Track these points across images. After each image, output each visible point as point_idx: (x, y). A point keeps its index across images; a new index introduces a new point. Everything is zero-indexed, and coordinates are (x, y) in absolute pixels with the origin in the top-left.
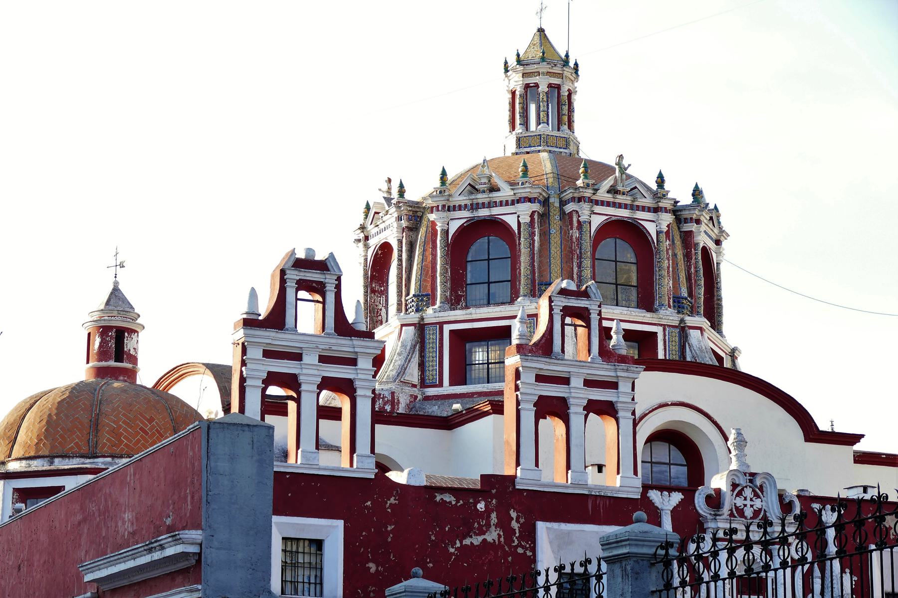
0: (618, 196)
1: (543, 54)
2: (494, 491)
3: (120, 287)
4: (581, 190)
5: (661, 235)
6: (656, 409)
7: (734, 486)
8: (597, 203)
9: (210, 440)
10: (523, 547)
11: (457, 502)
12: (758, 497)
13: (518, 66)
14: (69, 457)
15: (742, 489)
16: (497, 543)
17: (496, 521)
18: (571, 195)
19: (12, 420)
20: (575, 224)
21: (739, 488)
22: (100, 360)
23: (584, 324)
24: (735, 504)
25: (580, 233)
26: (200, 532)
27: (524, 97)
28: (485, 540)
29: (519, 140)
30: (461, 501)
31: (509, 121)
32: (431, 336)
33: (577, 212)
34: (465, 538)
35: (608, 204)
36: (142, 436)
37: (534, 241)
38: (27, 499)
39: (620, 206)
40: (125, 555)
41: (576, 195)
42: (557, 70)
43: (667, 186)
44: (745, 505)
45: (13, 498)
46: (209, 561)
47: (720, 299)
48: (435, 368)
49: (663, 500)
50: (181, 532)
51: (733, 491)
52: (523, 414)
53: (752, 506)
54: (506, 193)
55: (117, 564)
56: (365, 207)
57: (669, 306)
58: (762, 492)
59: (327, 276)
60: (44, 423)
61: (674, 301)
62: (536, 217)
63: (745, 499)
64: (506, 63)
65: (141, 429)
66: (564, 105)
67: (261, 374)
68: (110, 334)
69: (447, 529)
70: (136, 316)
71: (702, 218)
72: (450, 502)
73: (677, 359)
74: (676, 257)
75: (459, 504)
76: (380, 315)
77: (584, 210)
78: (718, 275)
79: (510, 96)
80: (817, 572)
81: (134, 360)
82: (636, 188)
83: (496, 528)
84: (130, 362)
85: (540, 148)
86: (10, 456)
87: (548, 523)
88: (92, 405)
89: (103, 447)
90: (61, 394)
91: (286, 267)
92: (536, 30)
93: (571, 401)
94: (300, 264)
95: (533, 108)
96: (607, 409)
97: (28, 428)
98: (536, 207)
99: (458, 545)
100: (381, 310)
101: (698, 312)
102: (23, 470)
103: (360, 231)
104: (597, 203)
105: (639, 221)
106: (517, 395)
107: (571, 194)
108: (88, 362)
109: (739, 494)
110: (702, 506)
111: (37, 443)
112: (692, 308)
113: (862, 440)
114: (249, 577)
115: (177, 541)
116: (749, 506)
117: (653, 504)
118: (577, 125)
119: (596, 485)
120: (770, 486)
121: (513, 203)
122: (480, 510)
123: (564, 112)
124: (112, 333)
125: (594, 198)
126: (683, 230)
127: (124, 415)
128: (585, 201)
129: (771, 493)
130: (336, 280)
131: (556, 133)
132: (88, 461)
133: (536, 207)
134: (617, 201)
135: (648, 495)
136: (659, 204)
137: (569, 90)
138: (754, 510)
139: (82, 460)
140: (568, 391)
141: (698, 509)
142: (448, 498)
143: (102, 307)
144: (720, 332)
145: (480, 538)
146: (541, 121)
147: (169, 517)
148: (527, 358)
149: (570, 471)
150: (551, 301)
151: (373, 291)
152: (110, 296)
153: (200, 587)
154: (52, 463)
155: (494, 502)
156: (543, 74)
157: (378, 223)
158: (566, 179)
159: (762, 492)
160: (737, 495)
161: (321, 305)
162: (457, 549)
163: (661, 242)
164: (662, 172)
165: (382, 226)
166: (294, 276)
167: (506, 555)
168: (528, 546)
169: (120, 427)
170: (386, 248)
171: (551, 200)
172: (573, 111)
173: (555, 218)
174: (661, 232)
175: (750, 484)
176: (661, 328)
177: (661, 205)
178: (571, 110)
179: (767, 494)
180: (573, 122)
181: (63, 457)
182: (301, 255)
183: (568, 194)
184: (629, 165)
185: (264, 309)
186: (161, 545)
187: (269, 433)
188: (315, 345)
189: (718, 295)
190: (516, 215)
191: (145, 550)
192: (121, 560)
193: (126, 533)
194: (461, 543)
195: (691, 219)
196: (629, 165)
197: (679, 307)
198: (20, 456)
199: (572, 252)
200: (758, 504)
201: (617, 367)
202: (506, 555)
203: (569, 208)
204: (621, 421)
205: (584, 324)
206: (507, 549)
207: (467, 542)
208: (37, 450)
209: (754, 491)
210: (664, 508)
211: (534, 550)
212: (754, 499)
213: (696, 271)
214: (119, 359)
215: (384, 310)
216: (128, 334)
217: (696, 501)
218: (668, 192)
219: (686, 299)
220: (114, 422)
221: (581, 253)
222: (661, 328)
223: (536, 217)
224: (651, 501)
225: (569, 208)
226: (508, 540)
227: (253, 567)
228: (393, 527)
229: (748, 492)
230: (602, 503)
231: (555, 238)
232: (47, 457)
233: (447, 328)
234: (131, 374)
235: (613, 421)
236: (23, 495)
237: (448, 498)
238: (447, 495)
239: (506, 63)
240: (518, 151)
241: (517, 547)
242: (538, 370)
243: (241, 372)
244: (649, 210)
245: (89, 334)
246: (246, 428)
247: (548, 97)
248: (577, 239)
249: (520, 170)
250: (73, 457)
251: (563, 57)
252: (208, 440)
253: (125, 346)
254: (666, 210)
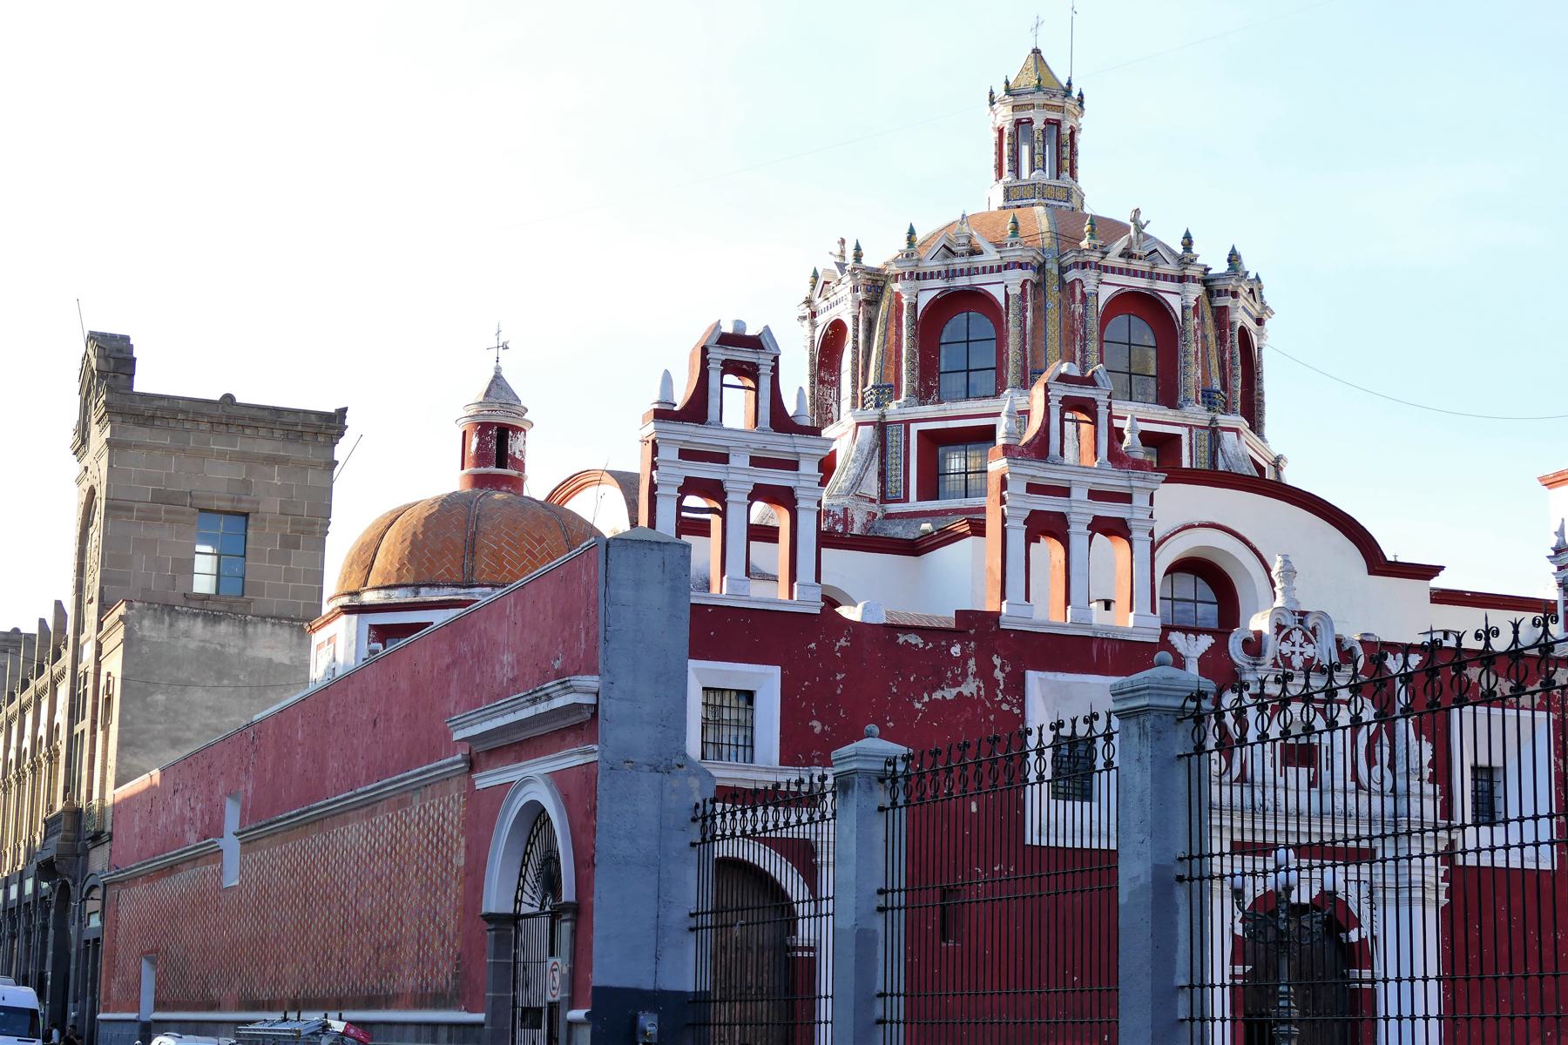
0: (1133, 261)
1: (1039, 81)
2: (972, 632)
3: (503, 374)
4: (1086, 253)
5: (1187, 310)
6: (1179, 531)
7: (1280, 628)
8: (1106, 269)
9: (609, 562)
10: (1008, 703)
11: (926, 644)
12: (1310, 642)
13: (1007, 97)
14: (438, 586)
15: (1290, 632)
16: (976, 697)
17: (975, 669)
18: (1073, 260)
19: (368, 539)
20: (1078, 296)
21: (1286, 631)
22: (478, 465)
23: (1089, 420)
24: (1280, 650)
25: (1085, 308)
26: (596, 678)
27: (1015, 136)
28: (960, 694)
29: (1007, 191)
30: (930, 644)
31: (995, 166)
32: (895, 438)
33: (1081, 281)
34: (934, 690)
35: (1121, 271)
36: (529, 561)
37: (1025, 318)
38: (386, 639)
39: (1135, 274)
40: (503, 707)
41: (1080, 260)
42: (1056, 102)
43: (1195, 250)
44: (1293, 653)
45: (369, 637)
46: (607, 715)
47: (1261, 394)
48: (899, 478)
49: (1188, 645)
50: (572, 678)
51: (1278, 634)
52: (1010, 533)
53: (1301, 654)
54: (991, 256)
55: (494, 718)
56: (811, 275)
57: (1197, 402)
58: (1315, 636)
59: (761, 356)
60: (407, 543)
61: (1203, 396)
62: (1028, 287)
63: (1293, 644)
64: (991, 93)
65: (529, 552)
66: (1066, 146)
67: (677, 480)
68: (490, 432)
69: (912, 679)
70: (523, 411)
71: (1240, 290)
72: (916, 645)
73: (1207, 468)
74: (1207, 339)
75: (927, 648)
76: (830, 412)
77: (1090, 278)
78: (1260, 363)
79: (996, 135)
81: (520, 465)
82: (1156, 250)
83: (974, 678)
84: (515, 468)
85: (1034, 201)
86: (365, 585)
87: (1041, 673)
88: (467, 521)
89: (481, 574)
90: (428, 508)
91: (709, 343)
92: (1030, 51)
93: (1072, 518)
94: (726, 340)
95: (1025, 151)
96: (1117, 529)
97: (388, 551)
98: (1028, 274)
99: (926, 699)
100: (831, 405)
101: (1234, 410)
102: (381, 602)
103: (805, 306)
104: (1106, 269)
105: (1159, 293)
106: (1003, 510)
107: (1074, 258)
108: (463, 468)
109: (1286, 638)
110: (1238, 654)
111: (399, 569)
112: (1225, 404)
113: (1441, 573)
114: (659, 736)
115: (568, 689)
116: (1297, 653)
117: (1176, 649)
118: (1081, 172)
119: (1102, 625)
120: (1326, 627)
121: (999, 269)
122: (955, 655)
123: (1064, 156)
124: (493, 432)
125: (1103, 263)
126: (1215, 305)
127: (506, 534)
128: (1090, 267)
129: (1327, 637)
130: (772, 361)
131: (1055, 182)
132: (462, 591)
133: (1028, 274)
134: (1131, 267)
135: (1169, 638)
136: (1186, 271)
137: (1071, 127)
138: (1305, 659)
139: (455, 590)
140: (1067, 505)
141: (1233, 656)
142: (914, 639)
143: (481, 399)
144: (1260, 435)
145: (955, 691)
146: (1036, 167)
147: (558, 659)
148: (1016, 461)
149: (1069, 607)
150: (1047, 390)
151: (822, 382)
152: (490, 385)
153: (596, 748)
154: (417, 593)
155: (972, 644)
156: (1039, 106)
157: (828, 296)
158: (1067, 239)
159: (1315, 636)
160: (1283, 640)
161: (753, 393)
162: (925, 704)
163: (1188, 320)
164: (1190, 232)
165: (833, 300)
166: (718, 355)
167: (987, 712)
168: (1015, 701)
169: (502, 549)
170: (837, 327)
171: (1048, 266)
172: (1077, 155)
173: (1053, 289)
174: (1188, 307)
175: (1300, 626)
176: (1186, 430)
177: (1188, 272)
178: (1073, 153)
179: (1321, 638)
180: (1077, 167)
181: (430, 585)
182: (728, 328)
183: (1070, 259)
184: (1148, 222)
185: (680, 398)
186: (547, 695)
187: (684, 552)
188: (745, 444)
189: (1259, 389)
190: (1003, 285)
191: (528, 701)
192: (498, 714)
193: (505, 679)
194: (930, 696)
195: (1226, 290)
196: (1148, 222)
197: (1209, 403)
198: (378, 585)
199: (1073, 332)
200: (1309, 651)
201: (1131, 475)
202: (987, 712)
203: (1071, 276)
204: (1136, 544)
205: (1089, 420)
206: (989, 705)
207: (938, 695)
208: (399, 577)
209: (1304, 634)
210: (1190, 655)
211: (1022, 706)
212: (1304, 644)
213: (1232, 358)
214: (501, 463)
215: (835, 405)
216: (513, 433)
217: (1230, 647)
218: (1197, 256)
219: (1218, 392)
220: (494, 543)
221: (1085, 333)
222: (1186, 430)
223: (1028, 287)
224: (1173, 645)
225: (1071, 276)
226: (991, 693)
227: (663, 723)
228: (843, 675)
229: (1297, 636)
230: (1110, 647)
231: (1052, 314)
232: (411, 586)
233: (914, 429)
234: (516, 483)
235: (1125, 543)
236: (383, 633)
237: (914, 639)
238: (913, 635)
239: (991, 93)
240: (1006, 204)
241: (1001, 702)
242: (1029, 478)
243: (652, 477)
244: (1173, 279)
245: (464, 433)
246: (655, 547)
247: (1044, 136)
248: (1081, 316)
249: (1008, 227)
250: (443, 587)
251: (1065, 85)
252: (607, 561)
253: (509, 448)
254: (1194, 280)
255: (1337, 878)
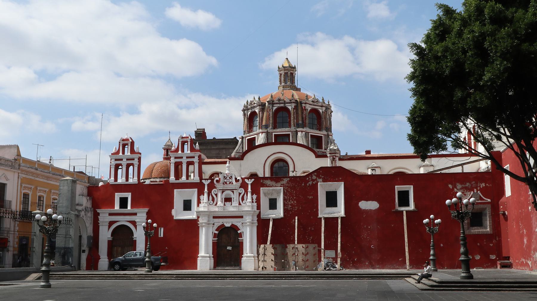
35: (278, 103)
51: (224, 178)
80: (245, 195)
98: (261, 107)
159: (232, 178)
176: (291, 132)
209: (229, 177)
229: (228, 178)
244: (289, 103)
255: (236, 222)
